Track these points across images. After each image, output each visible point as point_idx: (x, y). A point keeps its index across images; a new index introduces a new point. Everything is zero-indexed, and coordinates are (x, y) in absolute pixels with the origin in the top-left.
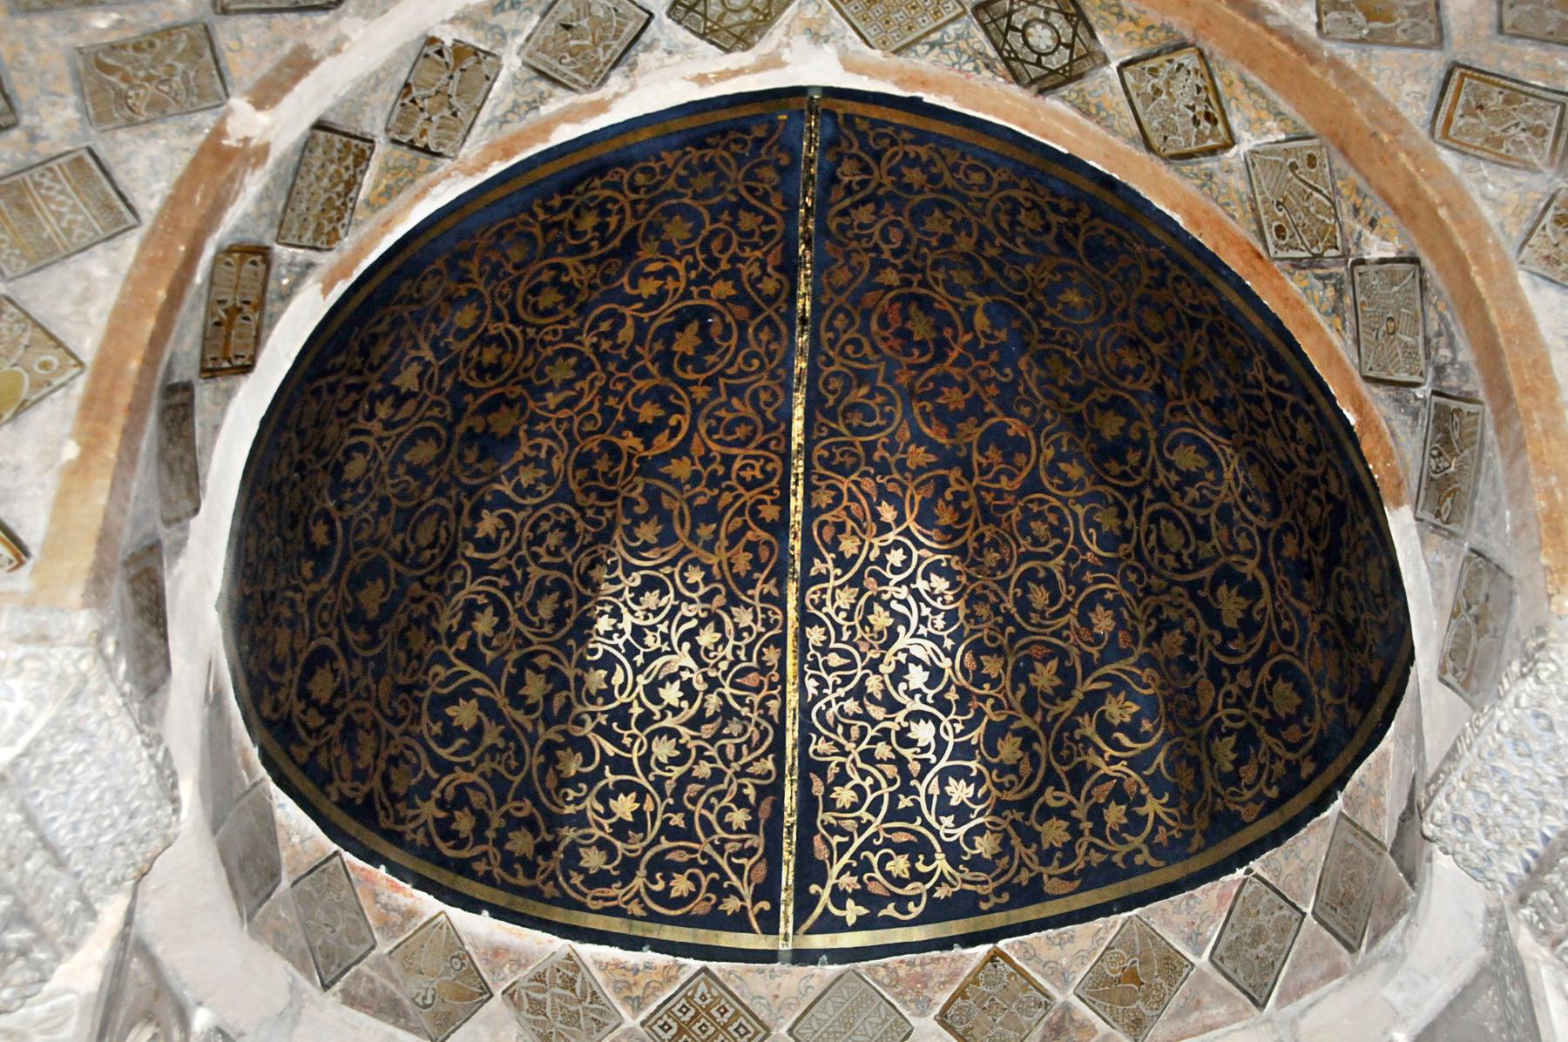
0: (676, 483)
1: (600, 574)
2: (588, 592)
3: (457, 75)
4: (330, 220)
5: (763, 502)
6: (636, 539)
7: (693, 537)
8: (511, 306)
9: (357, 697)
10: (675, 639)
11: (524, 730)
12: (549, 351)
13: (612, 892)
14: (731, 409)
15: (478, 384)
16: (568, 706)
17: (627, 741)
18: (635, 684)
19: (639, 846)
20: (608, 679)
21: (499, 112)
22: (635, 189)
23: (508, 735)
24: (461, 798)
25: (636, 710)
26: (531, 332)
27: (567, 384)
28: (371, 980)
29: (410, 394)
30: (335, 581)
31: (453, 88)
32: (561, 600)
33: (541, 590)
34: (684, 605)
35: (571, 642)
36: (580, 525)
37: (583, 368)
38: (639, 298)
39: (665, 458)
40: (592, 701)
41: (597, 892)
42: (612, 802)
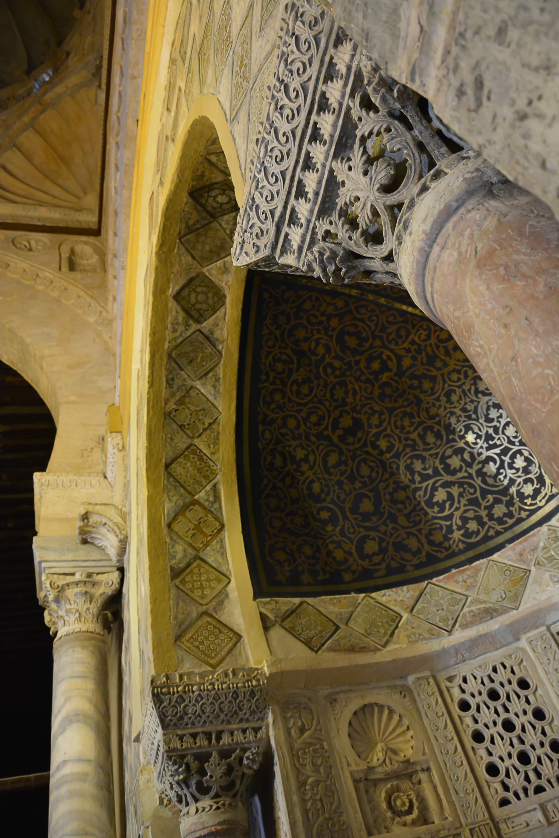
0: (412, 366)
1: (433, 411)
2: (438, 419)
3: (189, 405)
4: (207, 471)
5: (438, 336)
6: (427, 391)
7: (438, 369)
8: (299, 404)
9: (392, 534)
10: (475, 399)
11: (464, 477)
12: (328, 395)
13: (543, 494)
14: (391, 333)
15: (323, 427)
16: (472, 455)
17: (499, 443)
18: (481, 424)
19: (537, 469)
20: (474, 433)
21: (213, 392)
22: (274, 346)
23: (461, 485)
24: (465, 520)
25: (491, 431)
26: (316, 400)
27: (347, 392)
28: (472, 611)
29: (307, 456)
30: (345, 517)
31: (193, 408)
32: (432, 431)
33: (422, 437)
34: (464, 387)
35: (451, 437)
36: (408, 410)
37: (343, 384)
38: (324, 355)
39: (399, 366)
40: (476, 444)
41: (539, 498)
42: (515, 465)
